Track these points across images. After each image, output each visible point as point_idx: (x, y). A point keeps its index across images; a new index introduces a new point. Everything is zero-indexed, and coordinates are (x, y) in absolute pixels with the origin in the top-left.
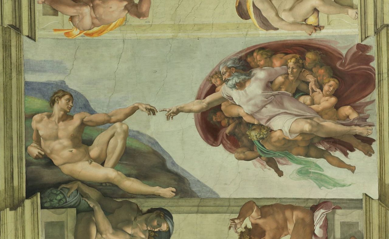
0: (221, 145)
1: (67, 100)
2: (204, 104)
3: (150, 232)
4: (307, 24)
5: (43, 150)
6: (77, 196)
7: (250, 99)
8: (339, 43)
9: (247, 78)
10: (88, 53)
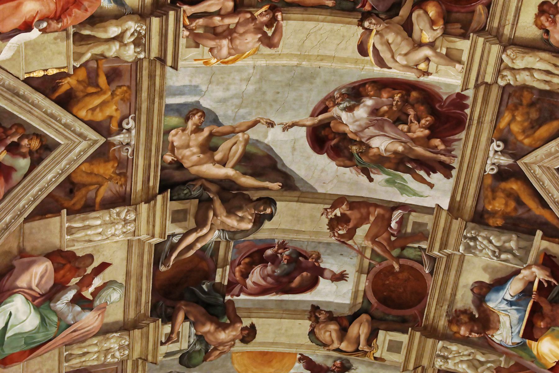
2: (316, 121)
4: (417, 69)
7: (356, 121)
8: (441, 89)
9: (357, 104)
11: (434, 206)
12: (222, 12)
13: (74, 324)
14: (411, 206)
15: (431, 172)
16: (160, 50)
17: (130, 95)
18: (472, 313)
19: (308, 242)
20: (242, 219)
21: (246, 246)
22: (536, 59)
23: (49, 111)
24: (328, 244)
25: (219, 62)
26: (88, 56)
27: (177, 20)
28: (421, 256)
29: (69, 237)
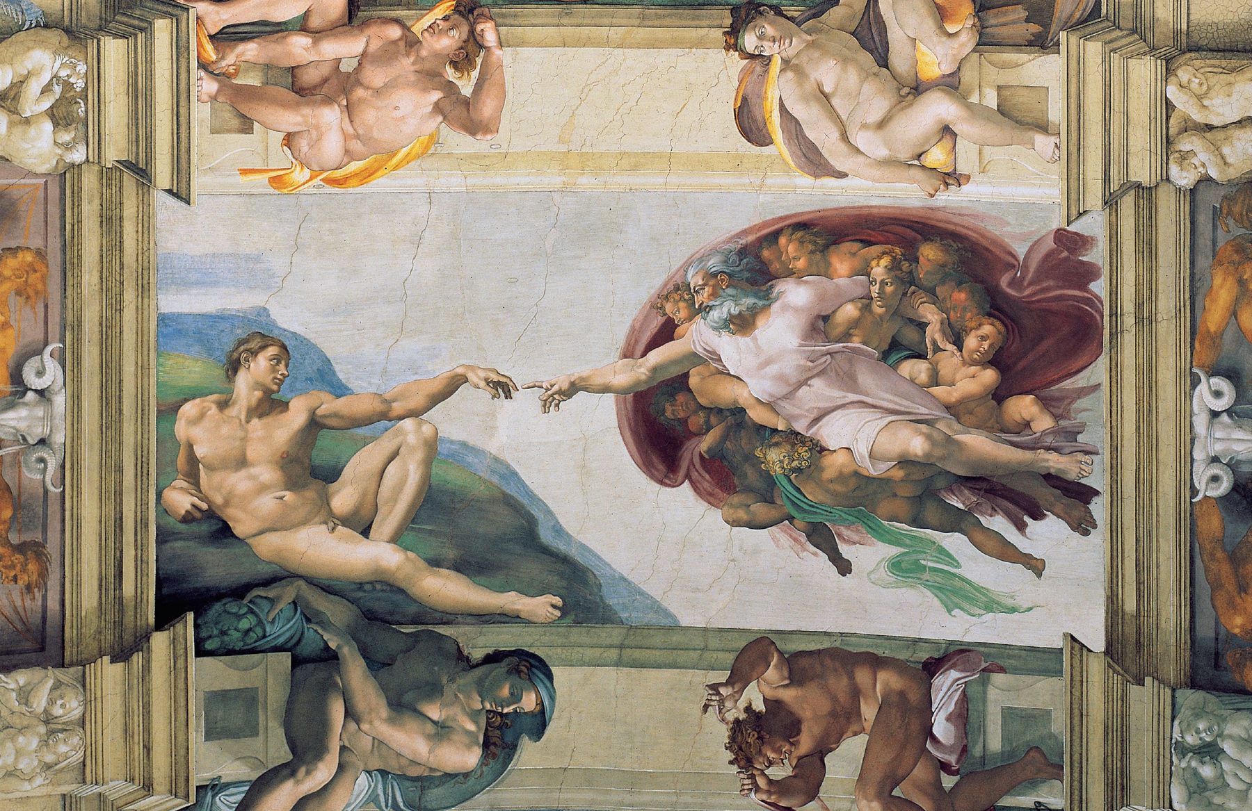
1: (271, 360)
3: (490, 716)
6: (294, 620)
10: (331, 231)
11: (1058, 643)
12: (315, 22)
25: (317, 181)
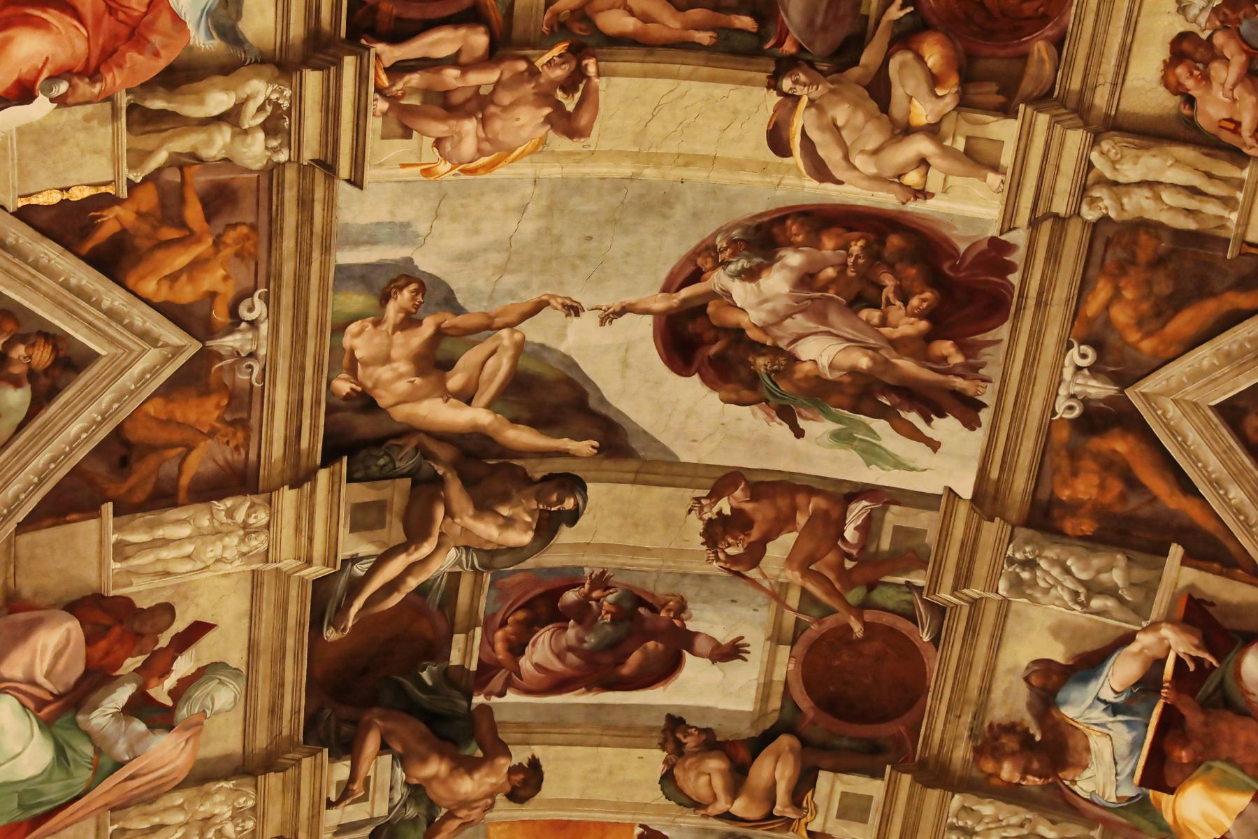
0: (696, 377)
2: (675, 301)
4: (901, 184)
5: (359, 383)
7: (766, 301)
8: (955, 228)
9: (766, 262)
10: (462, 205)
11: (940, 492)
12: (464, 59)
13: (131, 760)
14: (888, 491)
15: (933, 416)
16: (324, 144)
17: (256, 245)
18: (1027, 730)
19: (658, 572)
20: (509, 523)
21: (520, 583)
22: (1166, 161)
23: (73, 281)
24: (704, 577)
25: (456, 171)
26: (161, 157)
27: (362, 77)
28: (911, 603)
29: (118, 565)
